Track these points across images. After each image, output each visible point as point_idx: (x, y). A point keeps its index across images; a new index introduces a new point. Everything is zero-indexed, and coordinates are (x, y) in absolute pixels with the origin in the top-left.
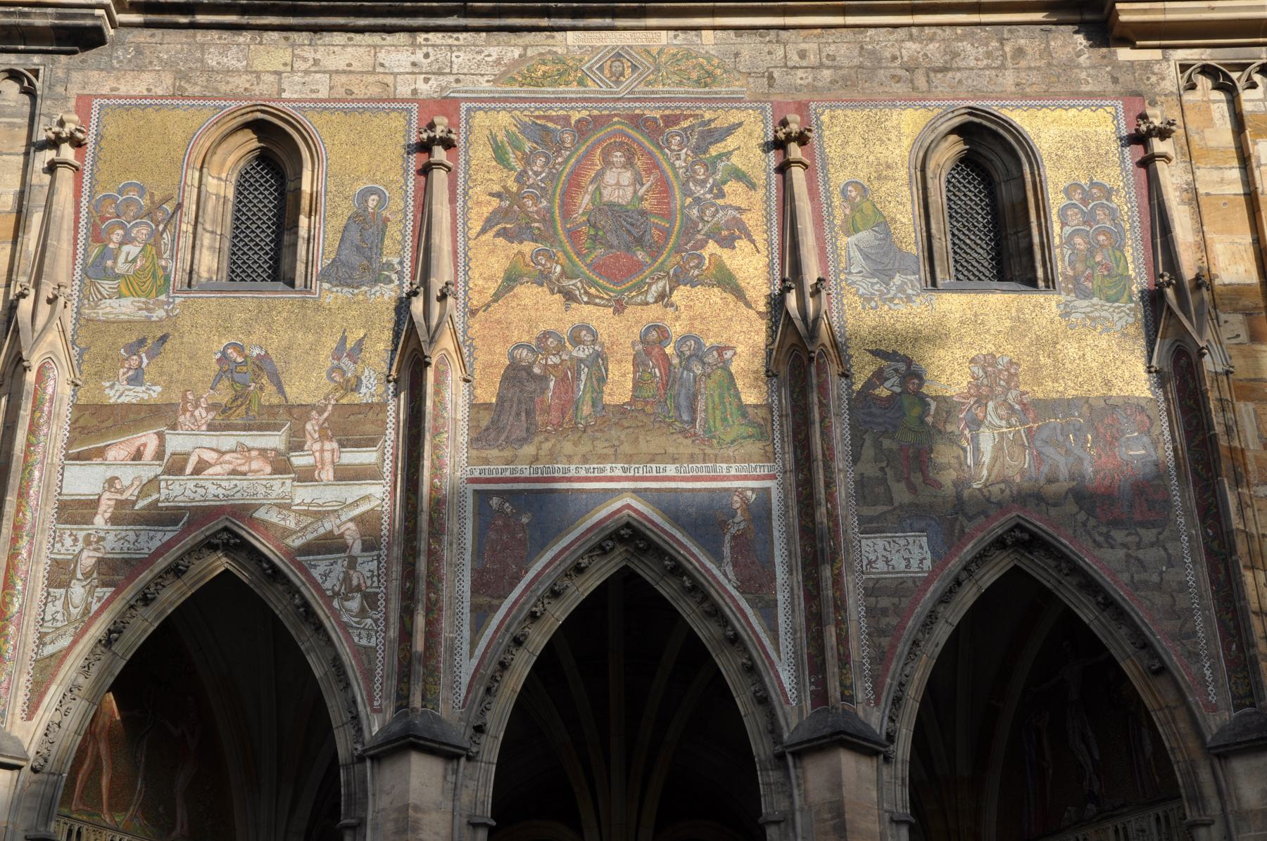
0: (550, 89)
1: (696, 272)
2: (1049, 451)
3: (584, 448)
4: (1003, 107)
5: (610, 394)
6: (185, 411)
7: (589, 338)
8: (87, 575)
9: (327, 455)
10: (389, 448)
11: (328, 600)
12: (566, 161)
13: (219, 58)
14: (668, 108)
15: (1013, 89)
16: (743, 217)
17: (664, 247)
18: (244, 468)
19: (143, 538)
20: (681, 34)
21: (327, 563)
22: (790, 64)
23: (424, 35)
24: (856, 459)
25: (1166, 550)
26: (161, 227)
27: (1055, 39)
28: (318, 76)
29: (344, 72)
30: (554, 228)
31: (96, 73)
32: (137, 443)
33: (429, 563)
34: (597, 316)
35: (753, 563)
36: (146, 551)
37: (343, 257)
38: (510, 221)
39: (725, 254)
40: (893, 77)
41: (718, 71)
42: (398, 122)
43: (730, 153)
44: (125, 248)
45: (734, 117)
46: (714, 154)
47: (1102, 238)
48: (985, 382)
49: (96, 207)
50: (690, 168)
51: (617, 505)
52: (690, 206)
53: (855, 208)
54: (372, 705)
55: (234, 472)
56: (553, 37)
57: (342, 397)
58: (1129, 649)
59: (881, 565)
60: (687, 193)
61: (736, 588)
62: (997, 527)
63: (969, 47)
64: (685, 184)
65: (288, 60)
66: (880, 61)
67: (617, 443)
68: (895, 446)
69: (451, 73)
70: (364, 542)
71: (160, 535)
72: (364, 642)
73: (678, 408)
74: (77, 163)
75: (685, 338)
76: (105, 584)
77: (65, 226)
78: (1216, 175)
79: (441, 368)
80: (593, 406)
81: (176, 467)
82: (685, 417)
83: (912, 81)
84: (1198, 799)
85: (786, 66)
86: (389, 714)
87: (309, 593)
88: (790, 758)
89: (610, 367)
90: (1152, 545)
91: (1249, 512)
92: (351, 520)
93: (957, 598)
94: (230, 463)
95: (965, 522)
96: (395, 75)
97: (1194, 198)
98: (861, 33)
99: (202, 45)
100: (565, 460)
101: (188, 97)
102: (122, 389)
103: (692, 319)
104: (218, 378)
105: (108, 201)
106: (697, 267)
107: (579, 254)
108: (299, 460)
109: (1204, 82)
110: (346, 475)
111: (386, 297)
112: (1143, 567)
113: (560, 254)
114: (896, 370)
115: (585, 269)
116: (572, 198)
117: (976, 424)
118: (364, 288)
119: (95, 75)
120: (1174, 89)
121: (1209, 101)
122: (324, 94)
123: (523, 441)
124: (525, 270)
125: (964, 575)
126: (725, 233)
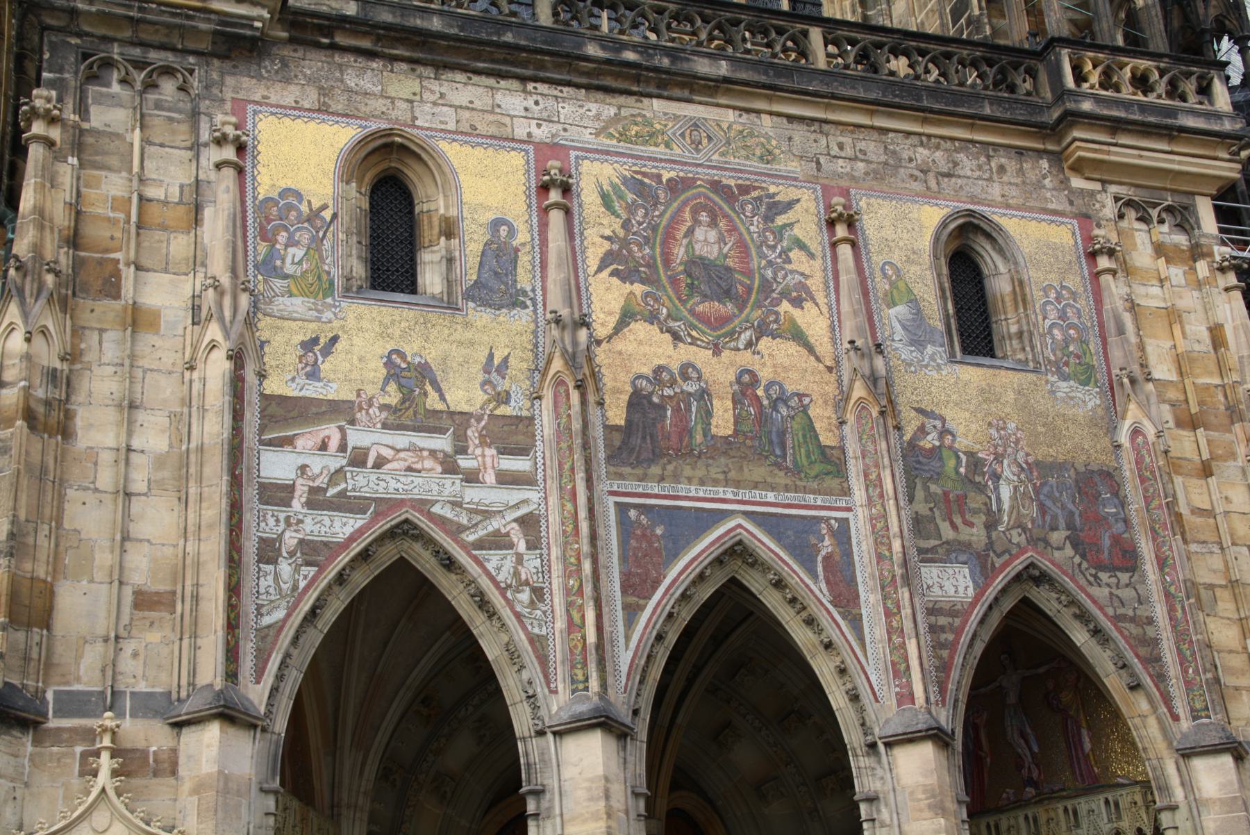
1: (775, 326)
2: (1048, 503)
3: (700, 472)
4: (993, 213)
6: (361, 409)
7: (694, 375)
8: (292, 554)
9: (488, 461)
11: (503, 592)
12: (661, 215)
13: (356, 80)
15: (999, 199)
18: (419, 466)
19: (337, 524)
20: (745, 116)
22: (832, 153)
24: (911, 499)
26: (321, 234)
28: (445, 109)
29: (468, 108)
30: (658, 274)
32: (322, 435)
34: (701, 357)
38: (619, 262)
39: (796, 313)
40: (912, 176)
44: (291, 250)
45: (793, 194)
47: (1072, 332)
50: (762, 234)
51: (731, 524)
52: (764, 268)
53: (892, 284)
54: (549, 687)
55: (409, 469)
57: (495, 408)
60: (762, 256)
61: (831, 602)
62: (1018, 565)
64: (759, 247)
65: (418, 90)
68: (939, 491)
70: (527, 542)
71: (351, 522)
72: (536, 631)
73: (771, 442)
75: (771, 384)
76: (308, 564)
80: (705, 435)
82: (778, 452)
84: (1165, 789)
85: (829, 154)
87: (485, 583)
88: (881, 747)
90: (1127, 586)
92: (515, 520)
95: (995, 559)
96: (512, 117)
97: (1133, 307)
99: (340, 66)
101: (333, 114)
103: (774, 366)
104: (386, 381)
105: (271, 204)
106: (776, 321)
107: (679, 299)
108: (464, 463)
109: (1131, 214)
110: (507, 479)
111: (524, 321)
112: (1123, 605)
114: (935, 427)
115: (686, 313)
117: (996, 477)
118: (504, 310)
119: (246, 82)
121: (1133, 229)
122: (451, 126)
124: (637, 309)
126: (794, 294)
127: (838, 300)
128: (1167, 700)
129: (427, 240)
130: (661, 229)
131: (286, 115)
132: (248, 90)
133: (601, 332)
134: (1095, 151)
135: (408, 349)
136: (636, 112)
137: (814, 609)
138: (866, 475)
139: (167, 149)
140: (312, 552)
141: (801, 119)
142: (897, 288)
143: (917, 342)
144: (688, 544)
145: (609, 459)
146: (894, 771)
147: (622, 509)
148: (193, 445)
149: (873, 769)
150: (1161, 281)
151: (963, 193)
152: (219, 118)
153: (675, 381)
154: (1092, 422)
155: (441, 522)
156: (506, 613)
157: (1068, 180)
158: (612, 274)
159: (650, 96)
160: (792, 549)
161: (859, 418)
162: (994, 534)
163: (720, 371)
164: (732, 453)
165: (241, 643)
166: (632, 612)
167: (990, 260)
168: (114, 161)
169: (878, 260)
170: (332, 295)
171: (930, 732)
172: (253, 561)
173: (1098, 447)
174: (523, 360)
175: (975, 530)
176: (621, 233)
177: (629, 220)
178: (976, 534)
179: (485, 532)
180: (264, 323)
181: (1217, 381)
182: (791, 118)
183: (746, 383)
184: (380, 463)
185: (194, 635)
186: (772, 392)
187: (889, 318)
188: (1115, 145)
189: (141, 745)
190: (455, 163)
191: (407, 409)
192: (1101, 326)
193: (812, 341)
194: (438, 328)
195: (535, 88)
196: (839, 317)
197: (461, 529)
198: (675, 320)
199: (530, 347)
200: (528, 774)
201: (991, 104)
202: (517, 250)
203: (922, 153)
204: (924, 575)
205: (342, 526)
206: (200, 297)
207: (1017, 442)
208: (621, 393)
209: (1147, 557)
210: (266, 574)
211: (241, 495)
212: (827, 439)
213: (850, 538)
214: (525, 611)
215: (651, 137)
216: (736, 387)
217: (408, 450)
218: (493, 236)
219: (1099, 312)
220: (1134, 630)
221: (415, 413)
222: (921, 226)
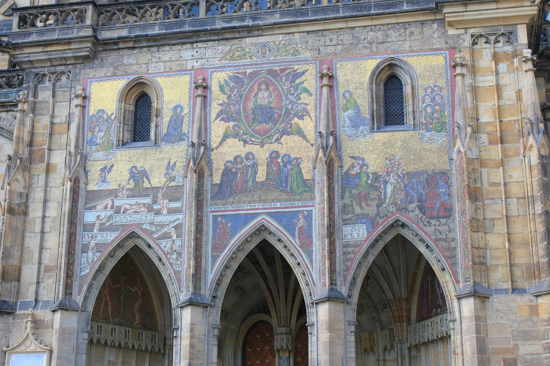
2: (411, 191)
3: (249, 199)
4: (404, 56)
7: (252, 157)
8: (93, 249)
9: (165, 205)
11: (166, 255)
12: (245, 90)
15: (408, 49)
17: (279, 121)
18: (139, 211)
19: (109, 236)
20: (287, 36)
23: (196, 44)
24: (342, 199)
25: (448, 226)
27: (425, 27)
28: (160, 63)
29: (169, 61)
34: (255, 149)
38: (225, 115)
39: (300, 122)
40: (364, 47)
41: (300, 49)
43: (303, 82)
44: (99, 134)
47: (437, 107)
49: (90, 119)
50: (289, 89)
51: (260, 218)
53: (348, 101)
54: (180, 290)
55: (136, 212)
56: (241, 41)
60: (287, 99)
62: (390, 221)
66: (359, 41)
68: (356, 192)
71: (113, 234)
72: (177, 269)
73: (281, 182)
75: (285, 155)
76: (98, 252)
79: (201, 172)
80: (253, 182)
81: (117, 211)
82: (284, 185)
83: (371, 48)
85: (325, 45)
90: (444, 225)
91: (479, 211)
92: (173, 227)
93: (377, 246)
95: (379, 220)
96: (186, 60)
106: (290, 128)
107: (248, 125)
108: (156, 207)
110: (171, 211)
114: (359, 164)
116: (247, 104)
117: (386, 182)
118: (176, 143)
119: (88, 71)
122: (162, 70)
124: (230, 133)
127: (320, 113)
128: (455, 275)
130: (244, 96)
131: (101, 81)
132: (88, 74)
133: (214, 145)
134: (456, 16)
135: (138, 165)
137: (293, 251)
140: (99, 247)
141: (313, 31)
143: (355, 126)
144: (241, 229)
145: (212, 197)
150: (493, 72)
153: (243, 161)
155: (145, 231)
156: (167, 263)
157: (447, 31)
158: (221, 120)
159: (245, 37)
160: (284, 227)
162: (381, 209)
168: (45, 112)
169: (341, 90)
173: (441, 161)
174: (182, 162)
176: (226, 101)
177: (230, 95)
178: (372, 210)
180: (89, 164)
181: (516, 118)
182: (308, 32)
184: (125, 211)
188: (467, 11)
189: (42, 318)
190: (162, 85)
195: (197, 46)
197: (153, 233)
201: (407, 3)
205: (111, 237)
207: (400, 164)
208: (220, 170)
212: (307, 176)
214: (174, 262)
220: (444, 244)
221: (139, 190)
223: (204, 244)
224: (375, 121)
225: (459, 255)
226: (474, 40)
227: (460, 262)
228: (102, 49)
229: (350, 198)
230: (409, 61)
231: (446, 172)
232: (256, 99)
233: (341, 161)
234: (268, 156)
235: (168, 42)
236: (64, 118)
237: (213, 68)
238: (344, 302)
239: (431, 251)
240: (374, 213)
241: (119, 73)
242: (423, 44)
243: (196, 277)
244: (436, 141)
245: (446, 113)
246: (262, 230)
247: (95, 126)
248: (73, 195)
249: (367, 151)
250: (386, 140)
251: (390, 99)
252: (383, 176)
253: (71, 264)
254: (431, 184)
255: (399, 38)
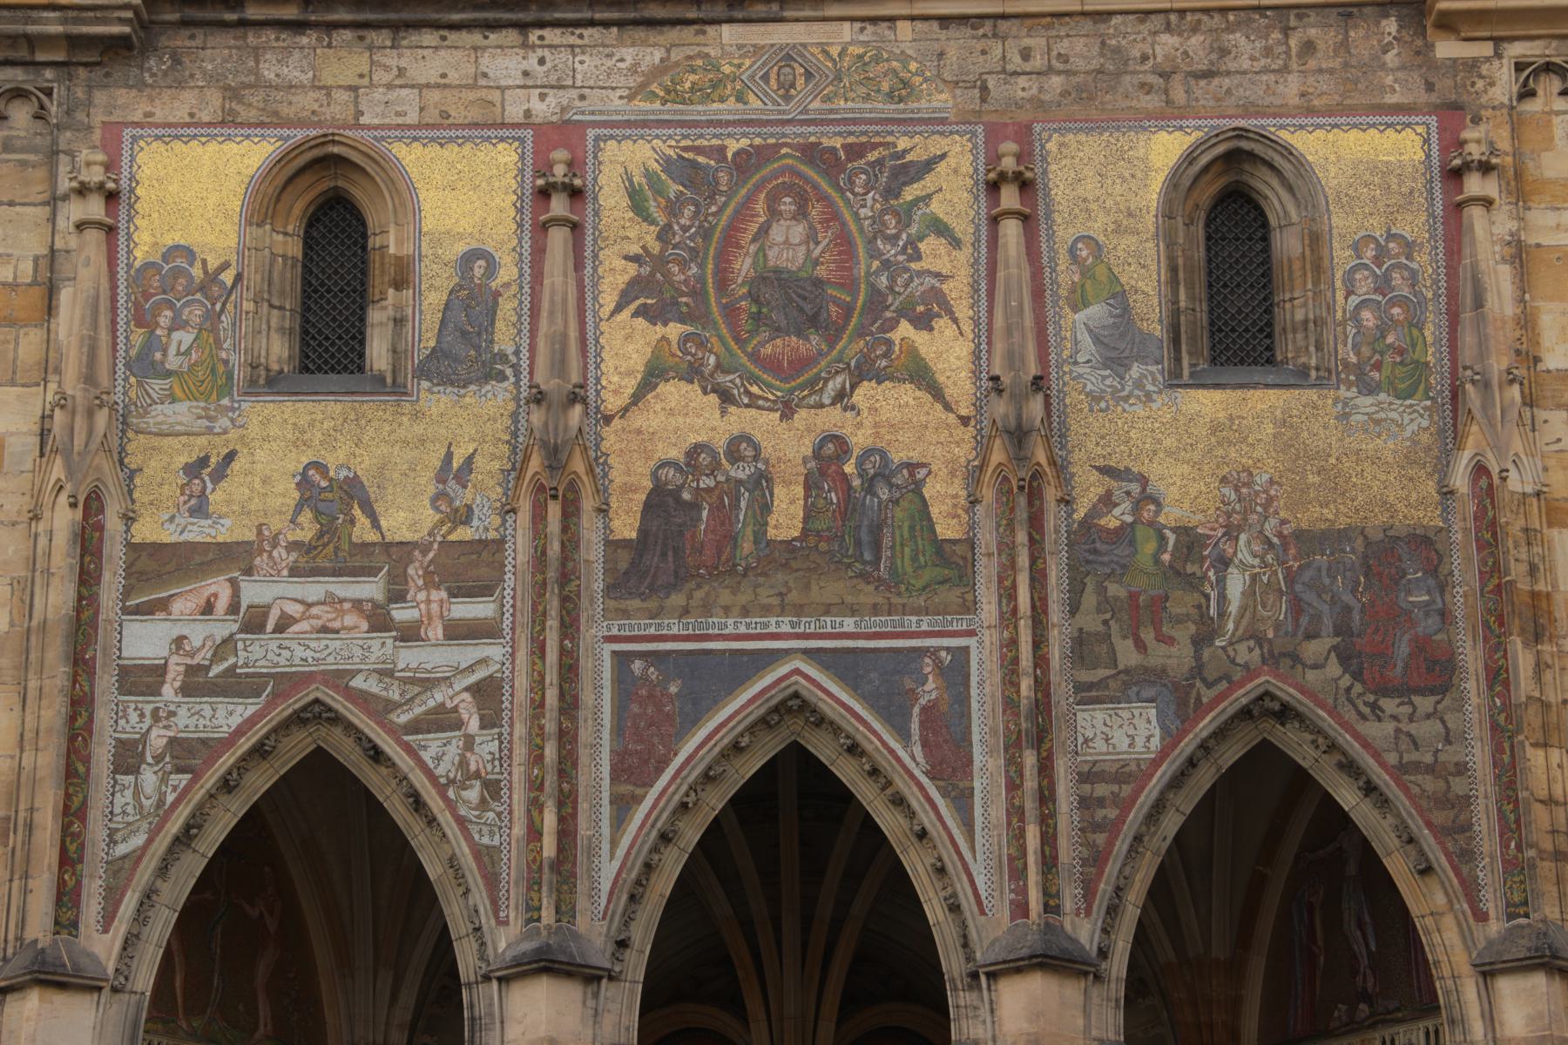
0: (700, 108)
1: (884, 363)
2: (1309, 596)
3: (744, 598)
4: (1282, 127)
5: (776, 527)
6: (261, 551)
7: (750, 453)
8: (158, 759)
10: (508, 598)
11: (442, 790)
13: (276, 68)
14: (851, 133)
16: (944, 287)
18: (337, 625)
19: (221, 713)
20: (870, 28)
21: (439, 743)
23: (539, 32)
24: (1074, 609)
25: (1443, 722)
26: (218, 307)
27: (1356, 27)
28: (404, 92)
29: (438, 86)
30: (706, 302)
31: (124, 91)
32: (206, 593)
33: (561, 747)
34: (761, 423)
35: (946, 741)
36: (225, 729)
37: (444, 346)
38: (651, 295)
39: (920, 338)
40: (1142, 85)
41: (917, 80)
42: (506, 156)
43: (929, 196)
44: (176, 336)
45: (937, 145)
46: (909, 198)
47: (1396, 311)
48: (1238, 507)
51: (784, 670)
53: (1086, 272)
54: (497, 917)
55: (324, 629)
56: (704, 33)
57: (450, 532)
58: (1392, 841)
59: (1100, 745)
60: (874, 254)
61: (926, 773)
62: (1242, 697)
63: (1243, 41)
64: (871, 241)
65: (365, 69)
66: (1126, 63)
67: (784, 590)
68: (1123, 593)
69: (573, 87)
71: (240, 709)
72: (486, 840)
73: (858, 543)
74: (109, 221)
75: (868, 452)
76: (180, 770)
77: (102, 309)
78: (1550, 219)
79: (570, 496)
80: (756, 542)
81: (254, 623)
82: (867, 556)
83: (1167, 94)
85: (1004, 71)
86: (515, 927)
87: (419, 780)
88: (983, 979)
89: (776, 491)
90: (1428, 716)
91: (1548, 676)
92: (467, 689)
93: (1192, 781)
94: (318, 617)
95: (1203, 690)
96: (502, 89)
97: (1520, 255)
98: (1104, 21)
99: (256, 48)
100: (721, 613)
101: (242, 125)
102: (183, 521)
103: (876, 425)
104: (299, 509)
105: (151, 272)
106: (886, 355)
107: (737, 339)
108: (400, 614)
110: (459, 632)
112: (1415, 744)
113: (714, 340)
114: (1128, 493)
115: (744, 360)
116: (729, 262)
117: (1224, 563)
118: (473, 387)
119: (123, 95)
120: (1506, 101)
122: (413, 118)
123: (672, 588)
124: (671, 361)
125: (1200, 754)
126: (921, 308)
127: (990, 311)
128: (1471, 889)
129: (377, 291)
131: (177, 137)
133: (612, 403)
135: (331, 460)
136: (690, 51)
137: (900, 783)
138: (1001, 580)
139: (18, 209)
140: (186, 754)
142: (1093, 277)
143: (1115, 362)
144: (716, 702)
145: (610, 590)
146: (997, 1013)
147: (622, 660)
148: (34, 623)
149: (976, 1008)
151: (1232, 101)
152: (84, 154)
153: (719, 464)
154: (1409, 459)
155: (363, 700)
156: (445, 818)
157: (1430, 47)
158: (636, 314)
159: (719, 22)
160: (871, 701)
161: (1000, 491)
162: (1206, 653)
163: (787, 441)
164: (794, 564)
165: (85, 881)
166: (623, 806)
167: (1277, 203)
169: (1065, 234)
170: (230, 394)
171: (1035, 961)
172: (106, 772)
173: (1414, 495)
174: (493, 457)
175: (1174, 650)
176: (655, 247)
177: (669, 226)
178: (1176, 656)
179: (424, 708)
180: (136, 444)
183: (829, 453)
185: (26, 876)
186: (868, 466)
187: (1074, 329)
190: (414, 173)
191: (325, 546)
192: (1453, 295)
193: (941, 379)
194: (375, 424)
195: (541, 38)
196: (989, 338)
198: (728, 372)
199: (507, 438)
200: (472, 1031)
202: (497, 294)
203: (1168, 43)
204: (1080, 722)
205: (226, 716)
206: (51, 417)
207: (1270, 500)
208: (635, 491)
209: (1472, 670)
210: (124, 787)
211: (92, 686)
212: (947, 529)
213: (967, 676)
215: (715, 87)
216: (812, 464)
217: (323, 603)
218: (462, 278)
219: (1452, 273)
220: (1430, 784)
221: (337, 548)
222: (1148, 169)
223: (584, 755)
224: (1184, 347)
225: (1484, 822)
226: (1525, 84)
227: (1486, 849)
228: (174, 17)
229: (1099, 611)
230: (1299, 145)
231: (1431, 534)
232: (762, 249)
233: (1068, 481)
234: (809, 452)
235: (435, 16)
236: (27, 268)
237: (604, 124)
238: (1086, 974)
239: (1384, 803)
240: (1186, 667)
241: (245, 114)
242: (1349, 86)
243: (560, 873)
244: (1394, 428)
245: (1427, 333)
246: (790, 710)
247: (157, 308)
248: (82, 556)
249: (1155, 452)
250: (1221, 415)
251: (1237, 271)
252: (1212, 541)
253: (75, 814)
254: (1380, 574)
255: (1263, 62)
